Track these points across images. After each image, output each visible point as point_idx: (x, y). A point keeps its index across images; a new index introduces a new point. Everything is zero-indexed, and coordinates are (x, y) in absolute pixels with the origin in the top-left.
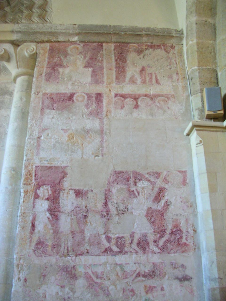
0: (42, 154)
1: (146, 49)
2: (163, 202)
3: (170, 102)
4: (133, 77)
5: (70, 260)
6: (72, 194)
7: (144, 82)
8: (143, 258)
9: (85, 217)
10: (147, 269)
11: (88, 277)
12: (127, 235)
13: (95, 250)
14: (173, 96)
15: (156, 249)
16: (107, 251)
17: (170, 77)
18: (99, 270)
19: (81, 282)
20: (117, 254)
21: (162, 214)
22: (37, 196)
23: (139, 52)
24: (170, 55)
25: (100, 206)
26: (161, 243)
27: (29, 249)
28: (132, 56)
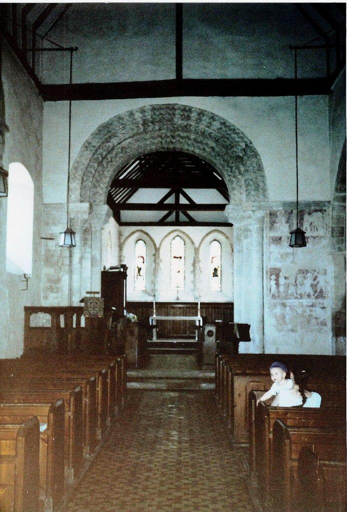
0: (272, 263)
1: (313, 212)
2: (316, 282)
3: (322, 240)
4: (306, 227)
5: (284, 301)
6: (283, 278)
7: (311, 230)
8: (309, 300)
9: (288, 286)
10: (311, 304)
11: (290, 306)
12: (303, 292)
13: (292, 297)
14: (324, 237)
15: (314, 298)
16: (296, 298)
17: (323, 227)
18: (294, 304)
19: (288, 308)
20: (299, 299)
21: (316, 285)
22: (271, 279)
23: (310, 214)
24: (324, 215)
25: (294, 283)
26: (316, 295)
27: (270, 298)
28: (306, 217)
